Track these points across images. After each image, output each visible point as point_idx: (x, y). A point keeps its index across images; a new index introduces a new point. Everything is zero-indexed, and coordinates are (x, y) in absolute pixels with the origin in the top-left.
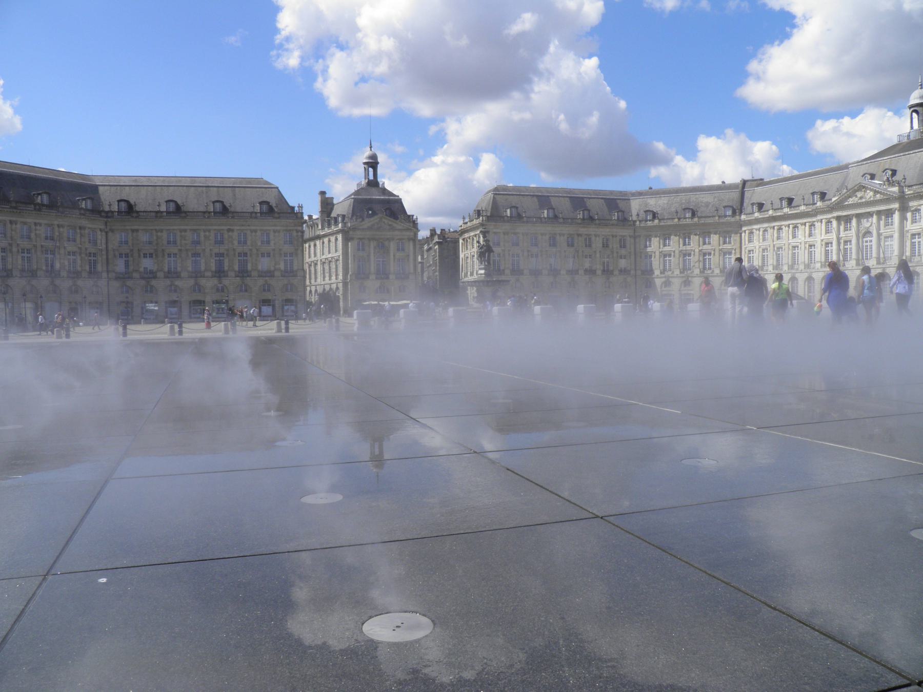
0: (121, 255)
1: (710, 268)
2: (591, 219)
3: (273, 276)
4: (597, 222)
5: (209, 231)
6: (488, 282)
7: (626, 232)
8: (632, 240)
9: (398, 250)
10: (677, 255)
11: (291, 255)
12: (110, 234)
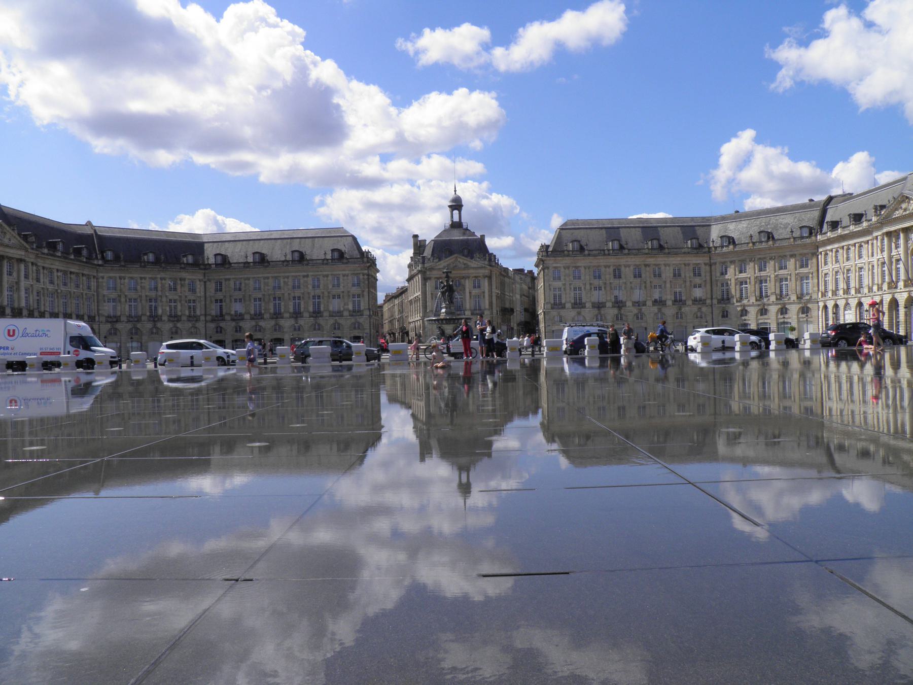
0: (216, 301)
1: (807, 294)
2: (661, 247)
3: (342, 316)
4: (667, 251)
5: (288, 277)
6: (450, 319)
7: (700, 260)
8: (708, 268)
9: (475, 287)
10: (753, 283)
11: (359, 296)
12: (208, 283)
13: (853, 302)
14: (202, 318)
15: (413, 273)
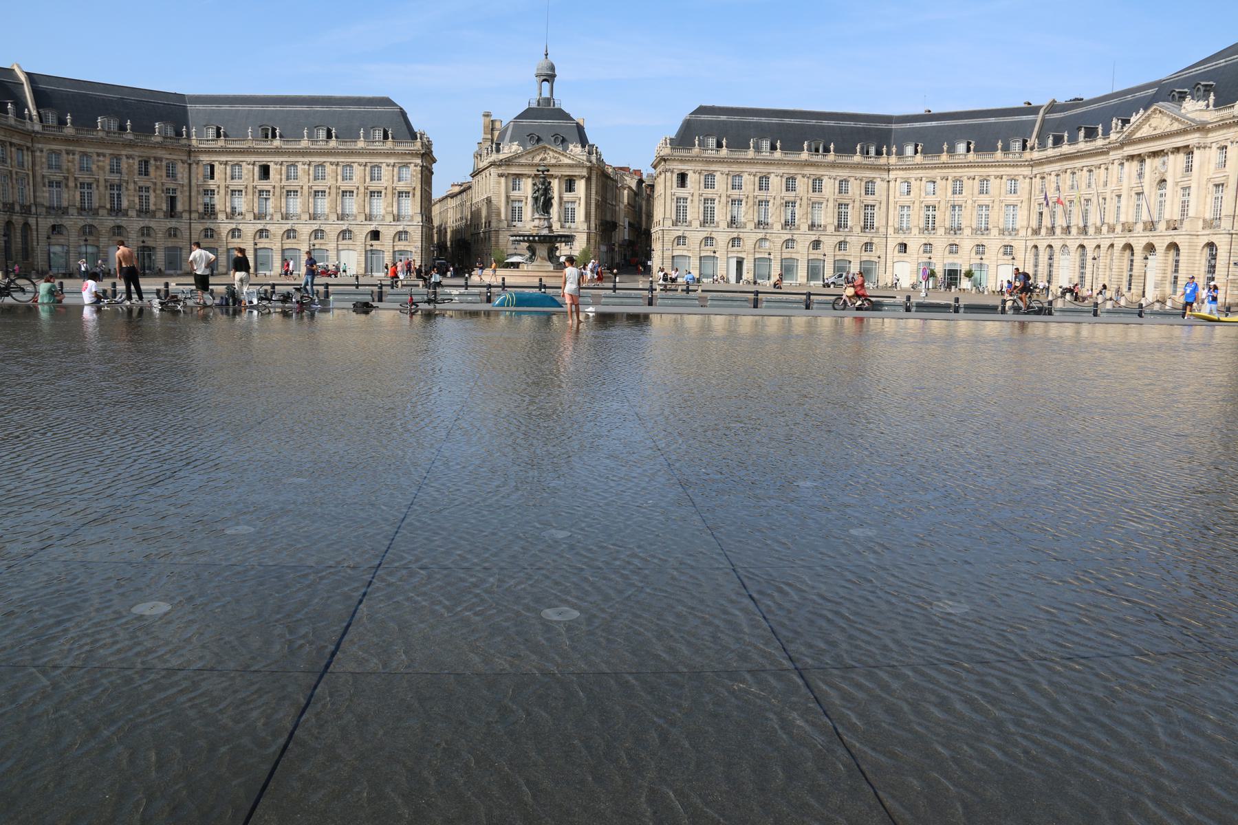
8: (885, 184)
12: (194, 166)
13: (1073, 244)
14: (186, 215)
15: (481, 165)
